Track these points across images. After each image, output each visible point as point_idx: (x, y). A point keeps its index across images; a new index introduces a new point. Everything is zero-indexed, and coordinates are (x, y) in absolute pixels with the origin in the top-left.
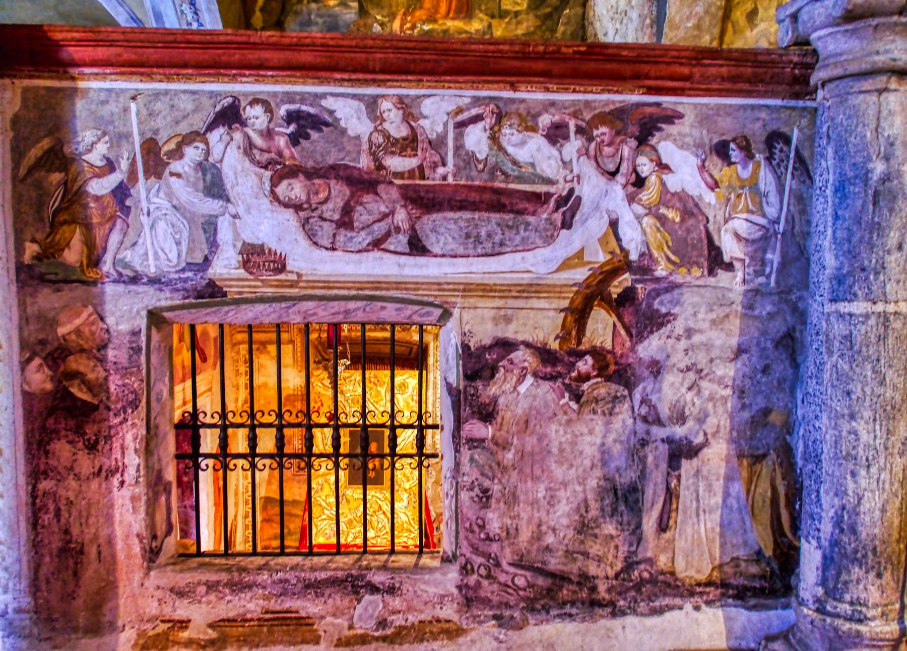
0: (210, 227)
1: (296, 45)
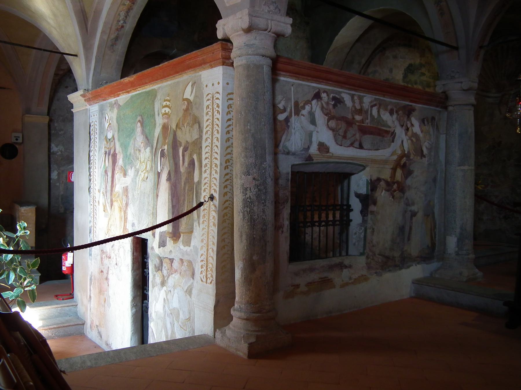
0: (310, 135)
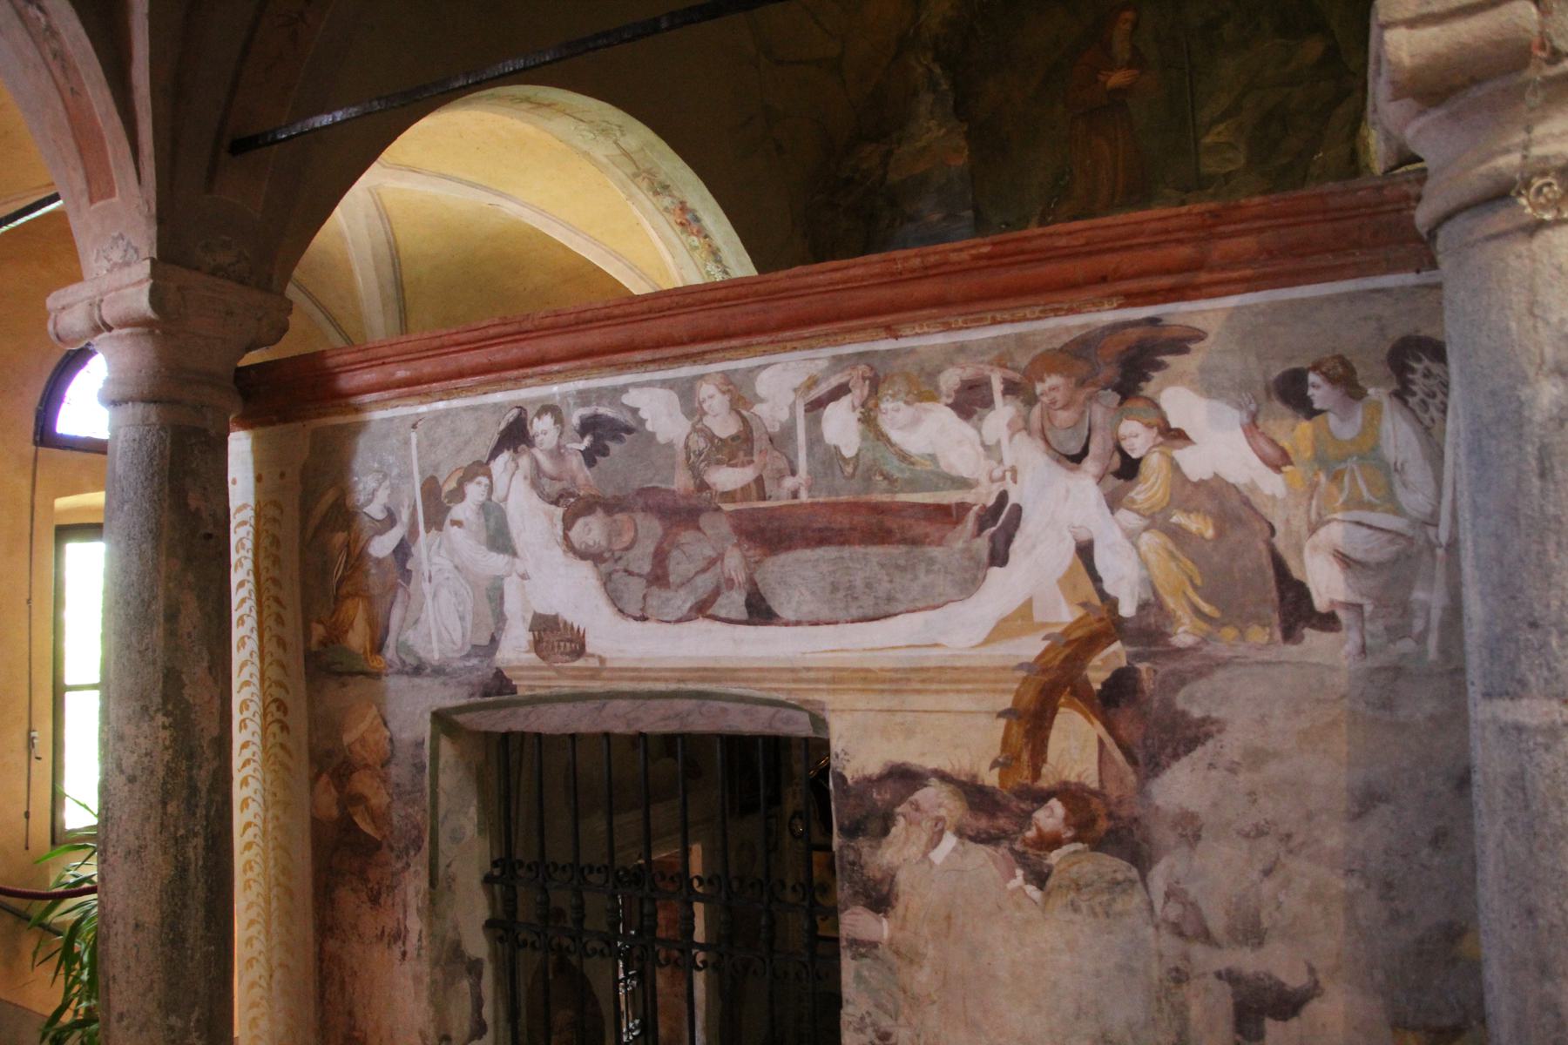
0: (496, 596)
1: (577, 324)
